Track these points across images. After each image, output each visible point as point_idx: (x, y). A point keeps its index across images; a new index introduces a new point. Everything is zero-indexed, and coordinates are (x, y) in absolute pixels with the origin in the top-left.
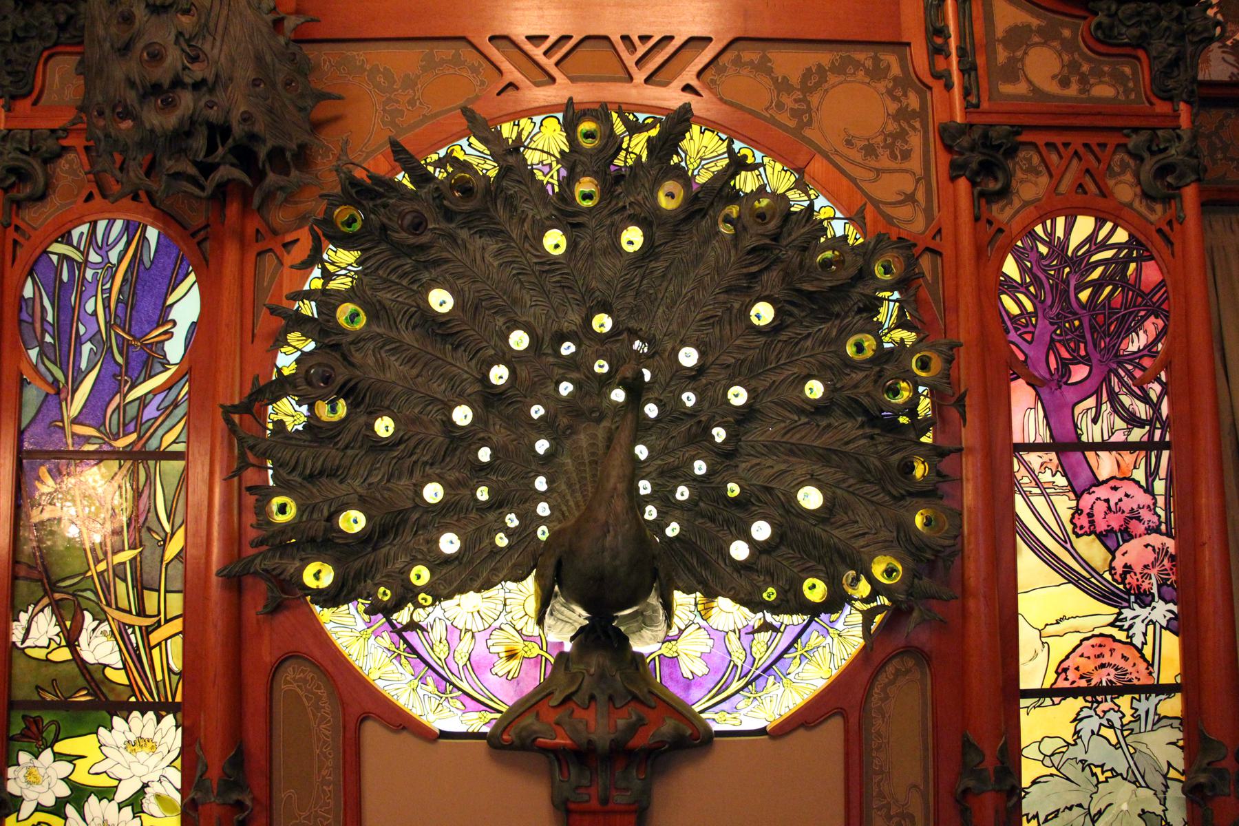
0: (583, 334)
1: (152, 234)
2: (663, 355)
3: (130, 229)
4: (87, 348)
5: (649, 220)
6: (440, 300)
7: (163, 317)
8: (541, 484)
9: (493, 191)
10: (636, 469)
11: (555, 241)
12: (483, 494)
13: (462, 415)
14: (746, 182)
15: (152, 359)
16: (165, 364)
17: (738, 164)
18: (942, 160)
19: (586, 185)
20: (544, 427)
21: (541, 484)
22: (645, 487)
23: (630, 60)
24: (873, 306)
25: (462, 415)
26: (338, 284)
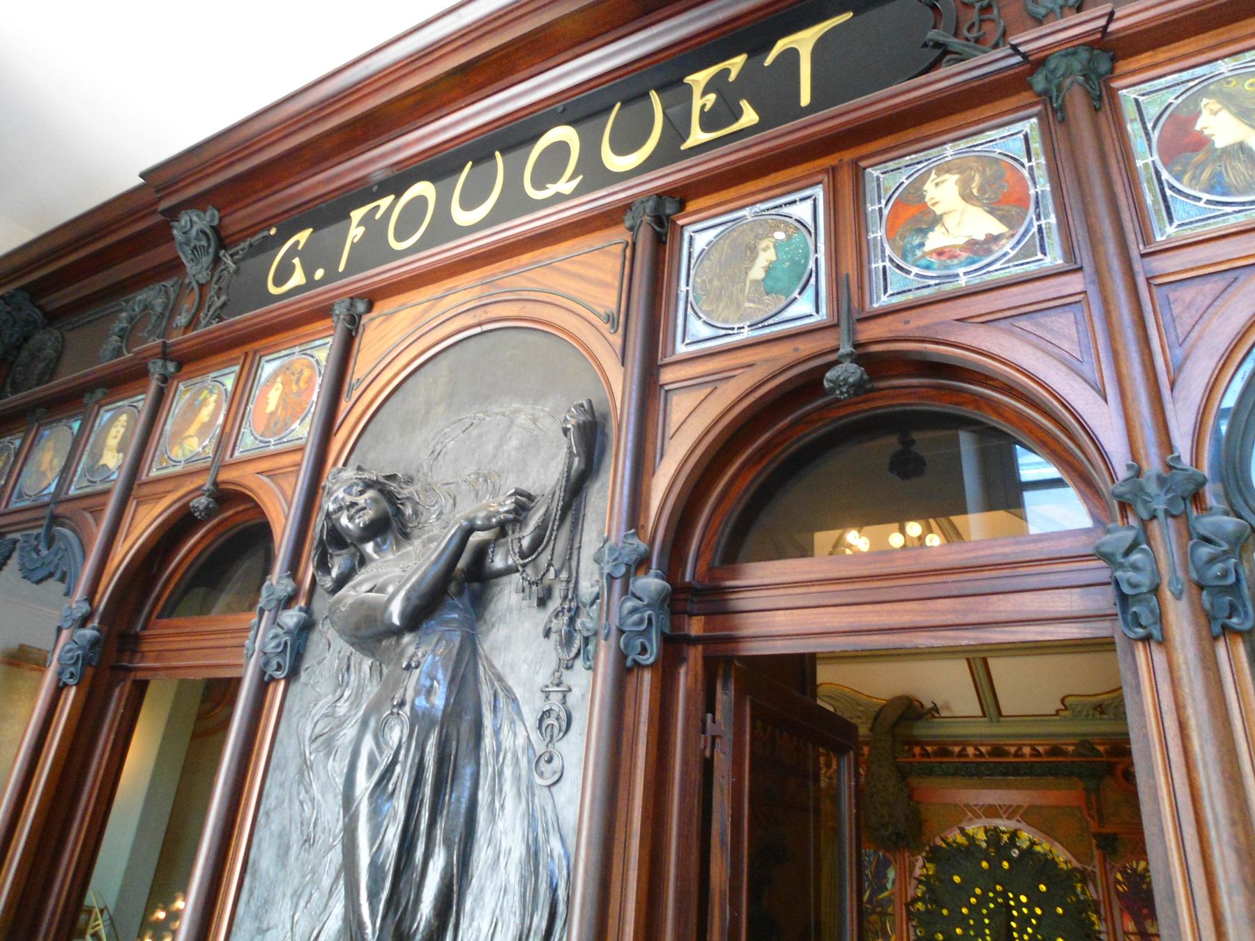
0: (994, 891)
1: (881, 854)
2: (1017, 899)
3: (876, 852)
4: (867, 884)
5: (1010, 859)
6: (957, 879)
7: (885, 876)
8: (987, 931)
9: (967, 848)
10: (1011, 929)
11: (985, 864)
12: (972, 933)
13: (965, 911)
14: (1038, 848)
15: (884, 888)
16: (887, 889)
17: (1033, 844)
18: (1094, 842)
19: (992, 850)
20: (988, 916)
21: (987, 931)
22: (1015, 935)
23: (1001, 812)
24: (1074, 888)
25: (965, 911)
26: (930, 873)
